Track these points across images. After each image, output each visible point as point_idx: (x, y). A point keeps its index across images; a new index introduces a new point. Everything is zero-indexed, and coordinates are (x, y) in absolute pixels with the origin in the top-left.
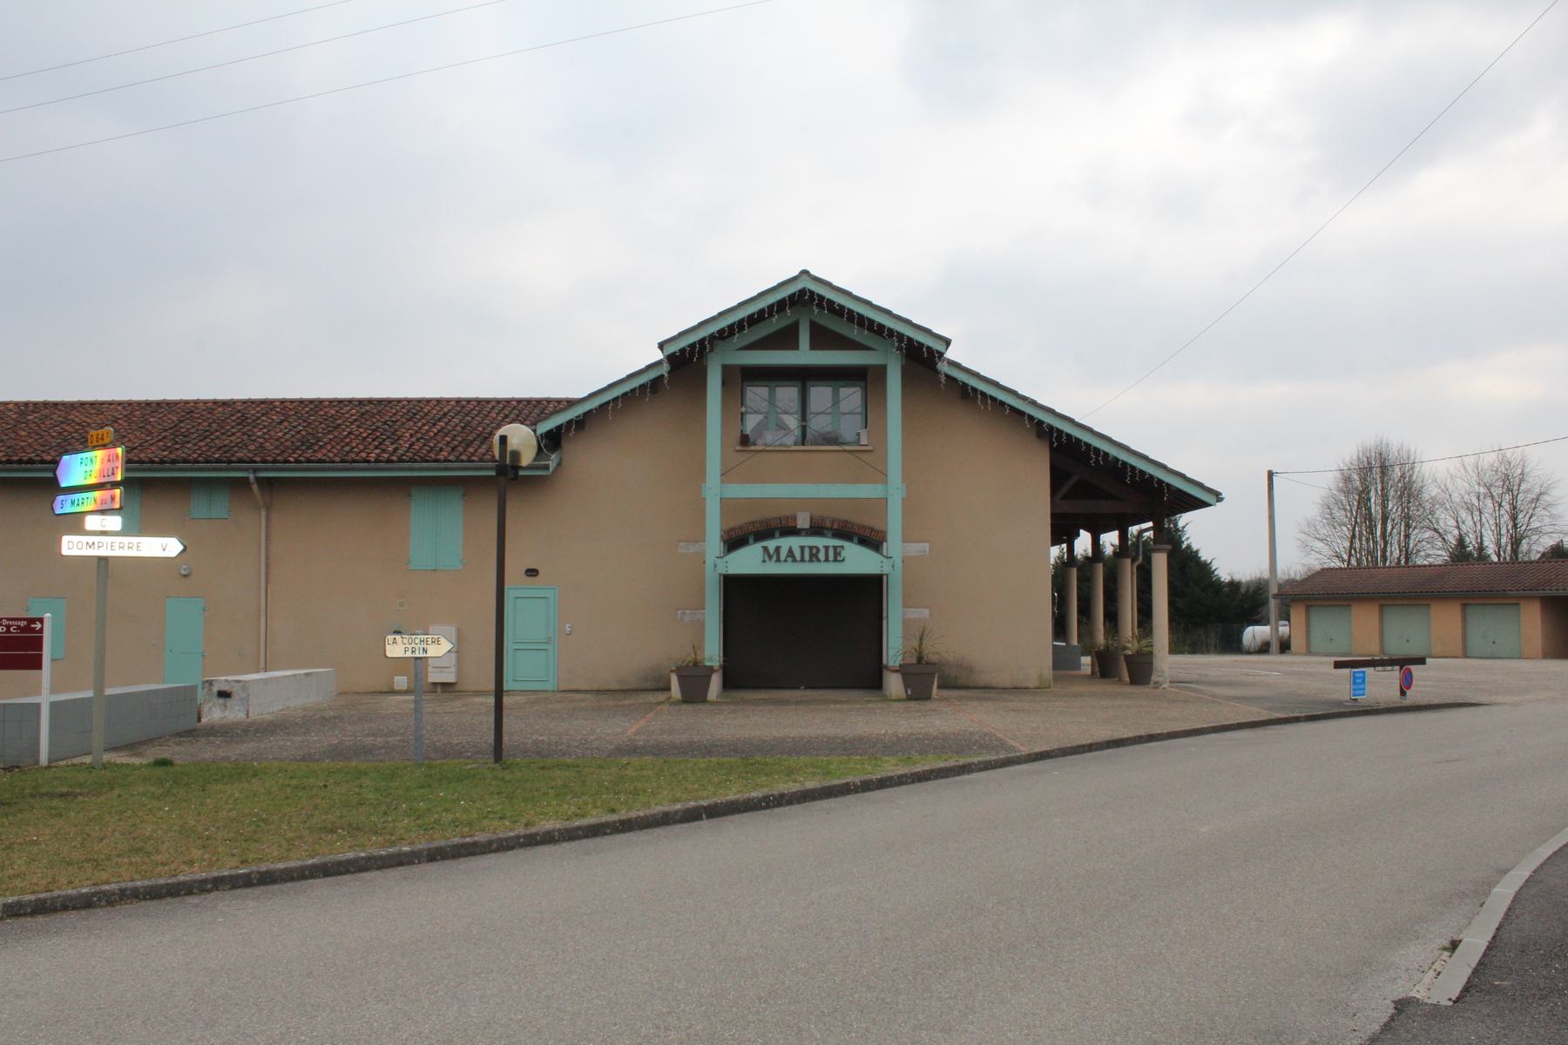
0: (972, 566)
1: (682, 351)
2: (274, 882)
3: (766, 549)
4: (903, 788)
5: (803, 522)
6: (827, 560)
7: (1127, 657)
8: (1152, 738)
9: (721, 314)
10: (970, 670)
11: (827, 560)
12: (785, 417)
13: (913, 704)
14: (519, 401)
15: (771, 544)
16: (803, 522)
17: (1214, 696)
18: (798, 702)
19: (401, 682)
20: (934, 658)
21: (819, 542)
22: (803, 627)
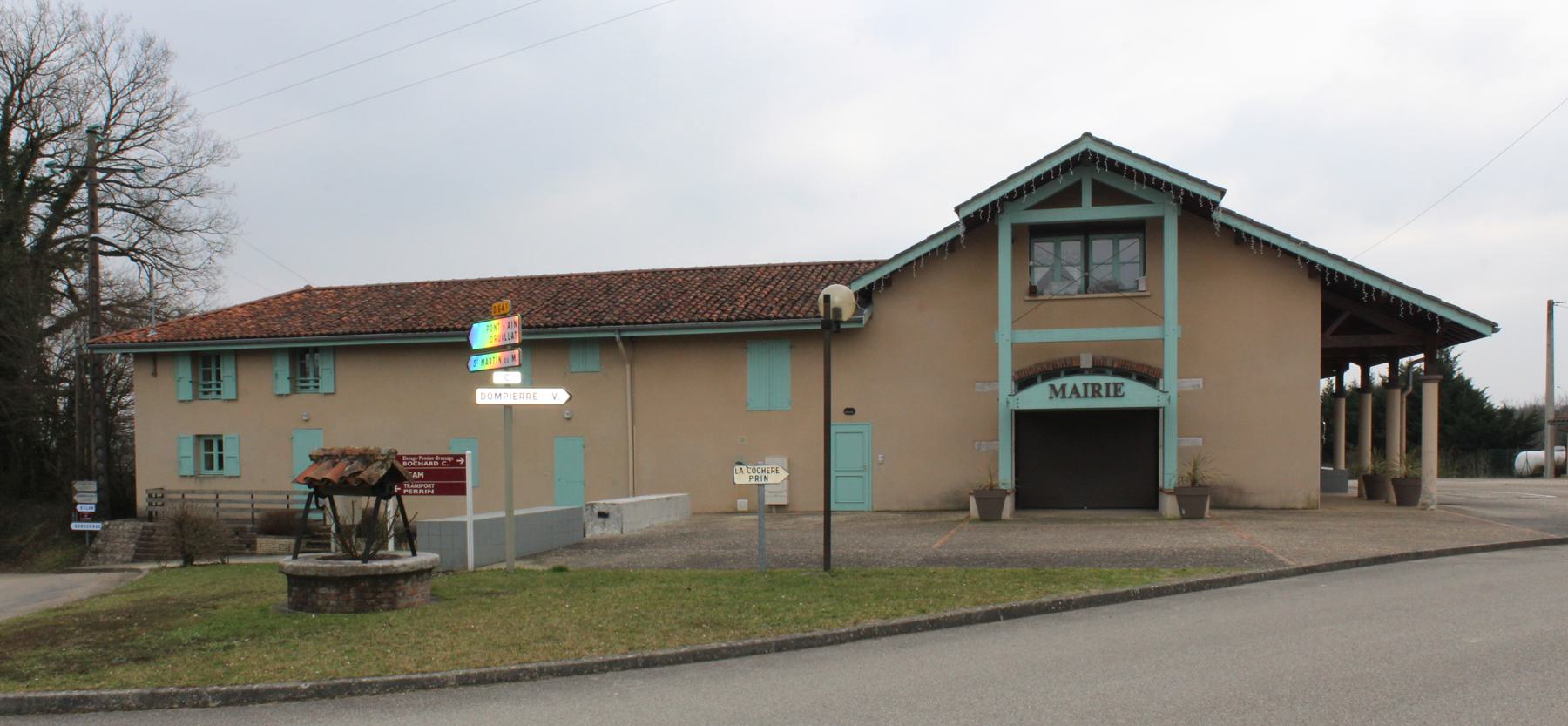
0: (1244, 399)
1: (976, 213)
2: (655, 665)
3: (1052, 387)
4: (1178, 596)
5: (1086, 362)
6: (1108, 395)
7: (1394, 481)
8: (1419, 555)
9: (1010, 178)
10: (1241, 492)
11: (1108, 395)
12: (1068, 269)
13: (1186, 522)
14: (835, 264)
15: (1058, 383)
16: (1086, 362)
17: (1484, 517)
18: (1085, 521)
19: (743, 504)
20: (1207, 482)
21: (1101, 380)
22: (1088, 458)
